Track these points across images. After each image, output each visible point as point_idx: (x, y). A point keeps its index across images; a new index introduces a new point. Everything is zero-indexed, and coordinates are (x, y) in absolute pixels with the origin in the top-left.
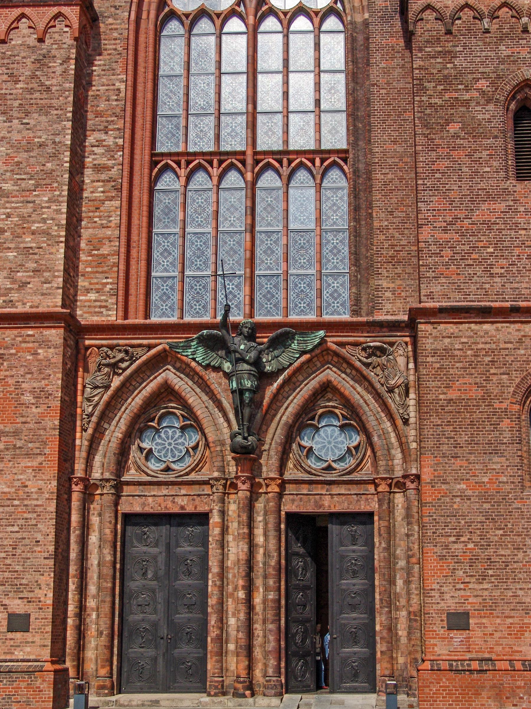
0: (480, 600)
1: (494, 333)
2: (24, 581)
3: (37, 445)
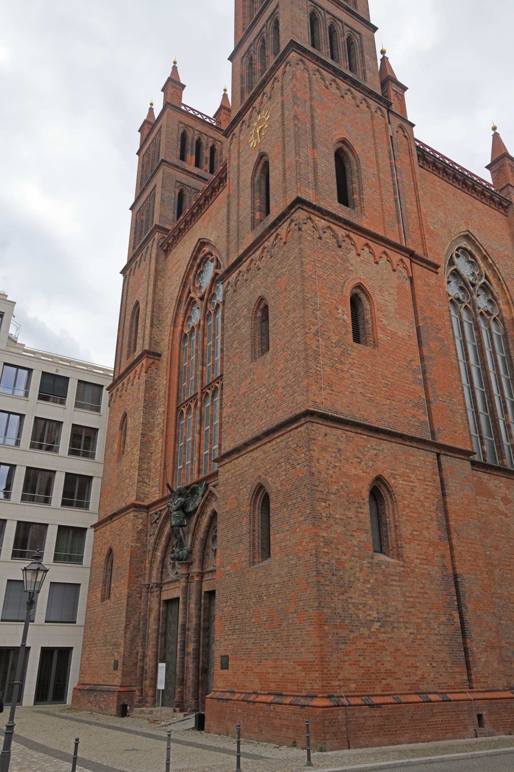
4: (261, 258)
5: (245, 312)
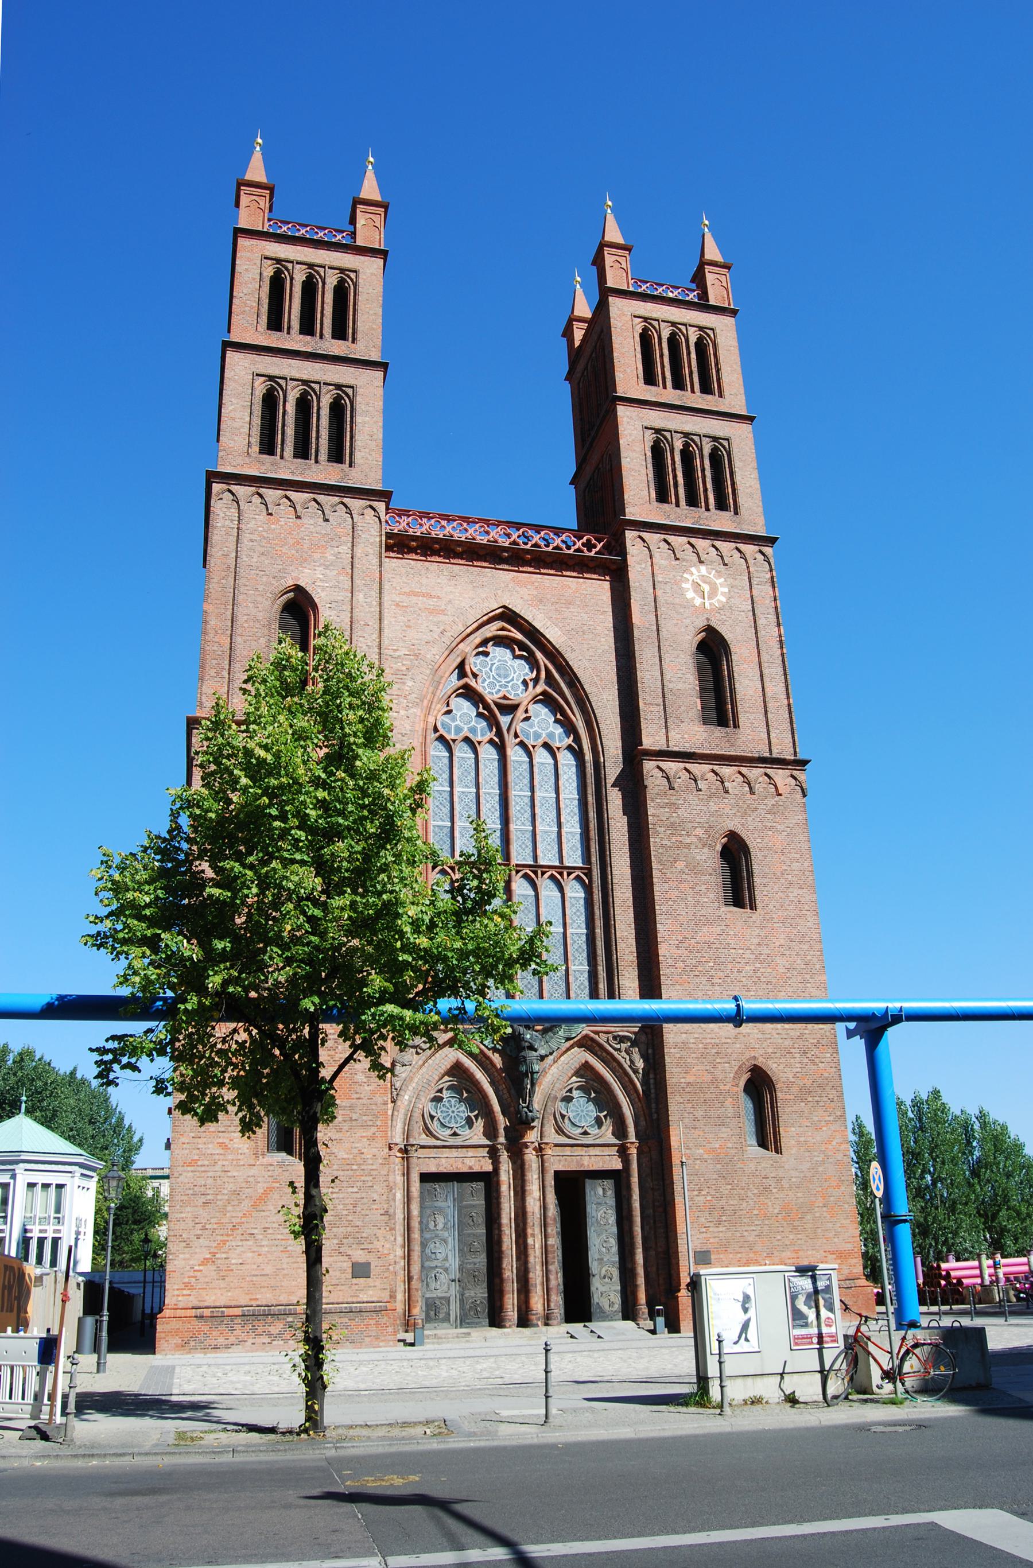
1: (718, 1030)
2: (364, 1235)
3: (370, 1118)
5: (699, 831)
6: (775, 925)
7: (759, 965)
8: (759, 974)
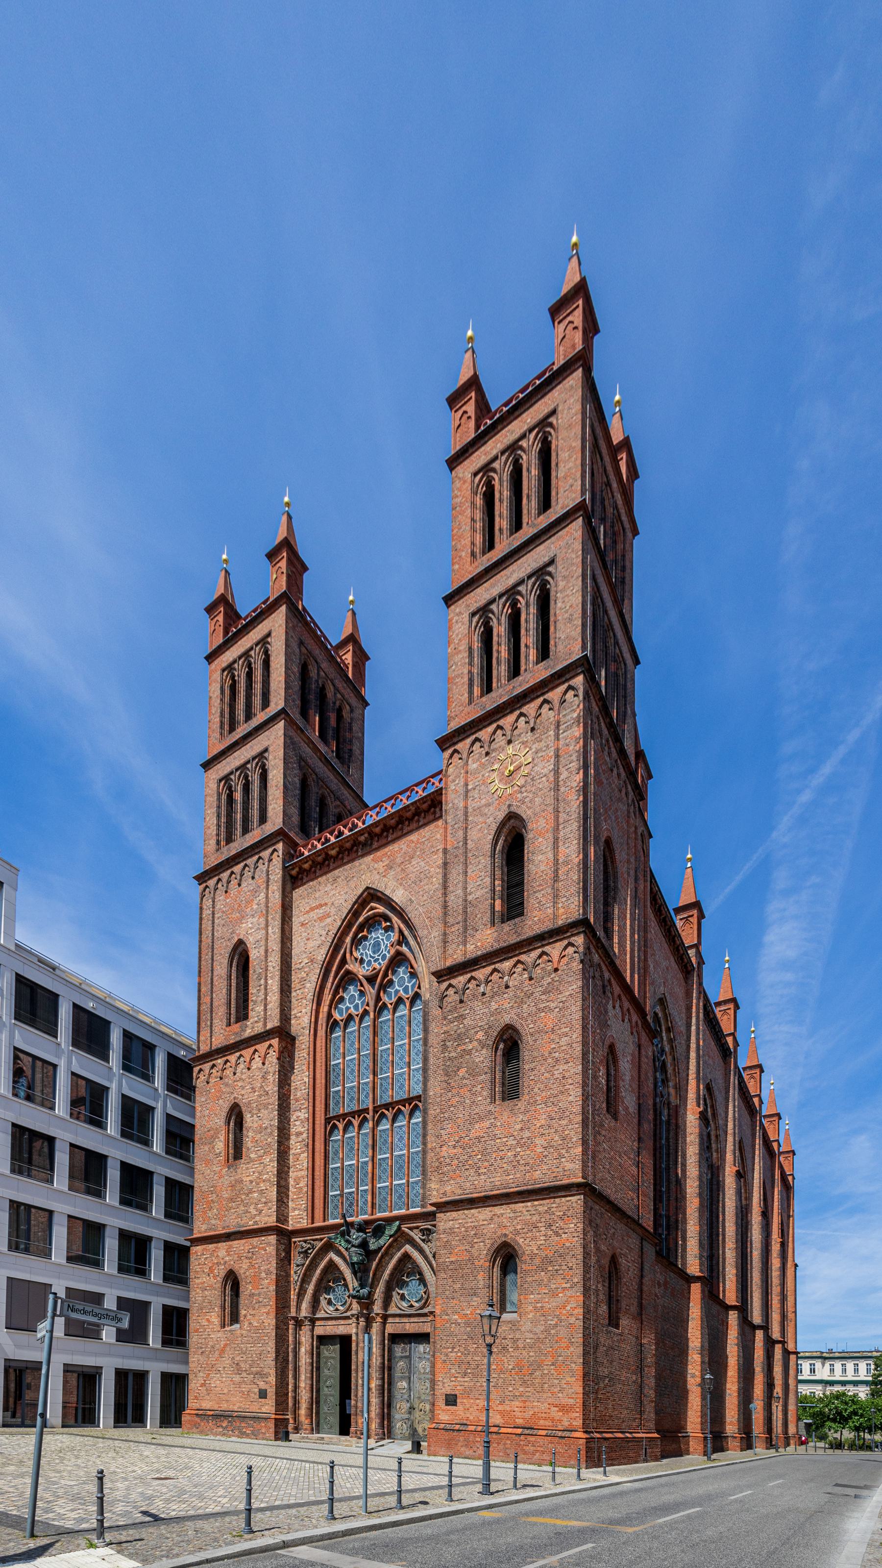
0: (462, 1388)
4: (511, 974)
6: (538, 1107)
7: (519, 1150)
8: (519, 1158)
